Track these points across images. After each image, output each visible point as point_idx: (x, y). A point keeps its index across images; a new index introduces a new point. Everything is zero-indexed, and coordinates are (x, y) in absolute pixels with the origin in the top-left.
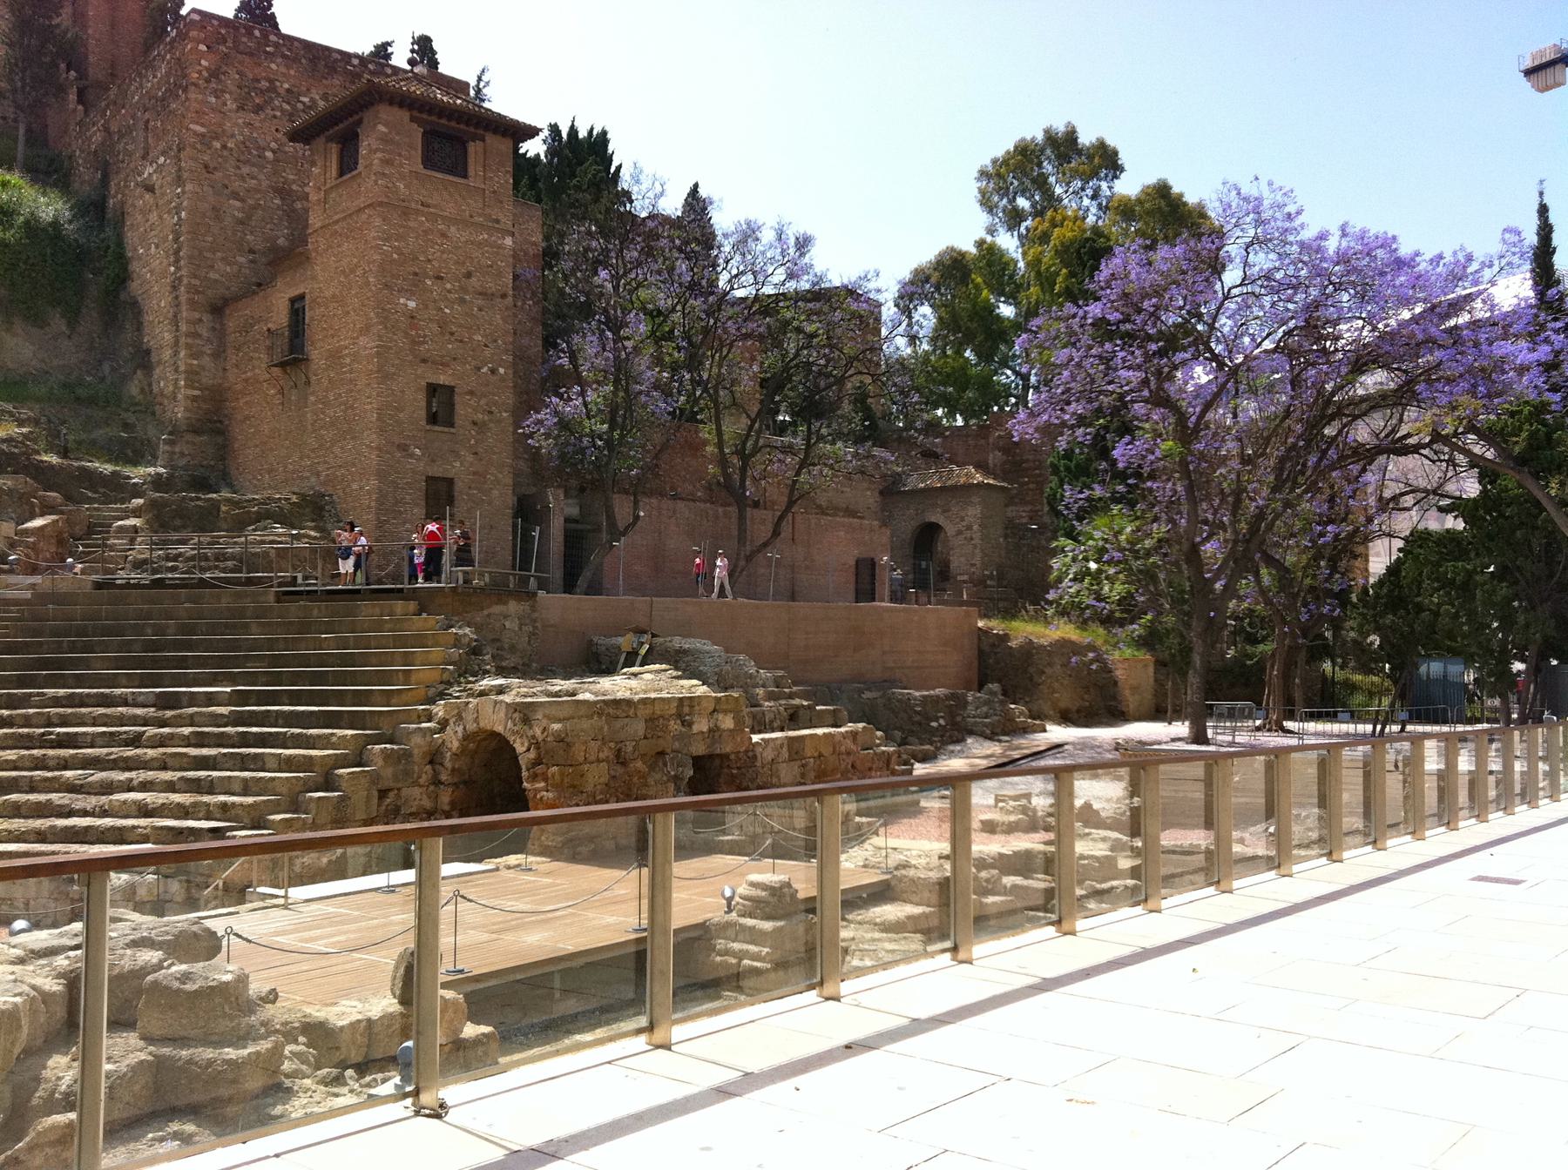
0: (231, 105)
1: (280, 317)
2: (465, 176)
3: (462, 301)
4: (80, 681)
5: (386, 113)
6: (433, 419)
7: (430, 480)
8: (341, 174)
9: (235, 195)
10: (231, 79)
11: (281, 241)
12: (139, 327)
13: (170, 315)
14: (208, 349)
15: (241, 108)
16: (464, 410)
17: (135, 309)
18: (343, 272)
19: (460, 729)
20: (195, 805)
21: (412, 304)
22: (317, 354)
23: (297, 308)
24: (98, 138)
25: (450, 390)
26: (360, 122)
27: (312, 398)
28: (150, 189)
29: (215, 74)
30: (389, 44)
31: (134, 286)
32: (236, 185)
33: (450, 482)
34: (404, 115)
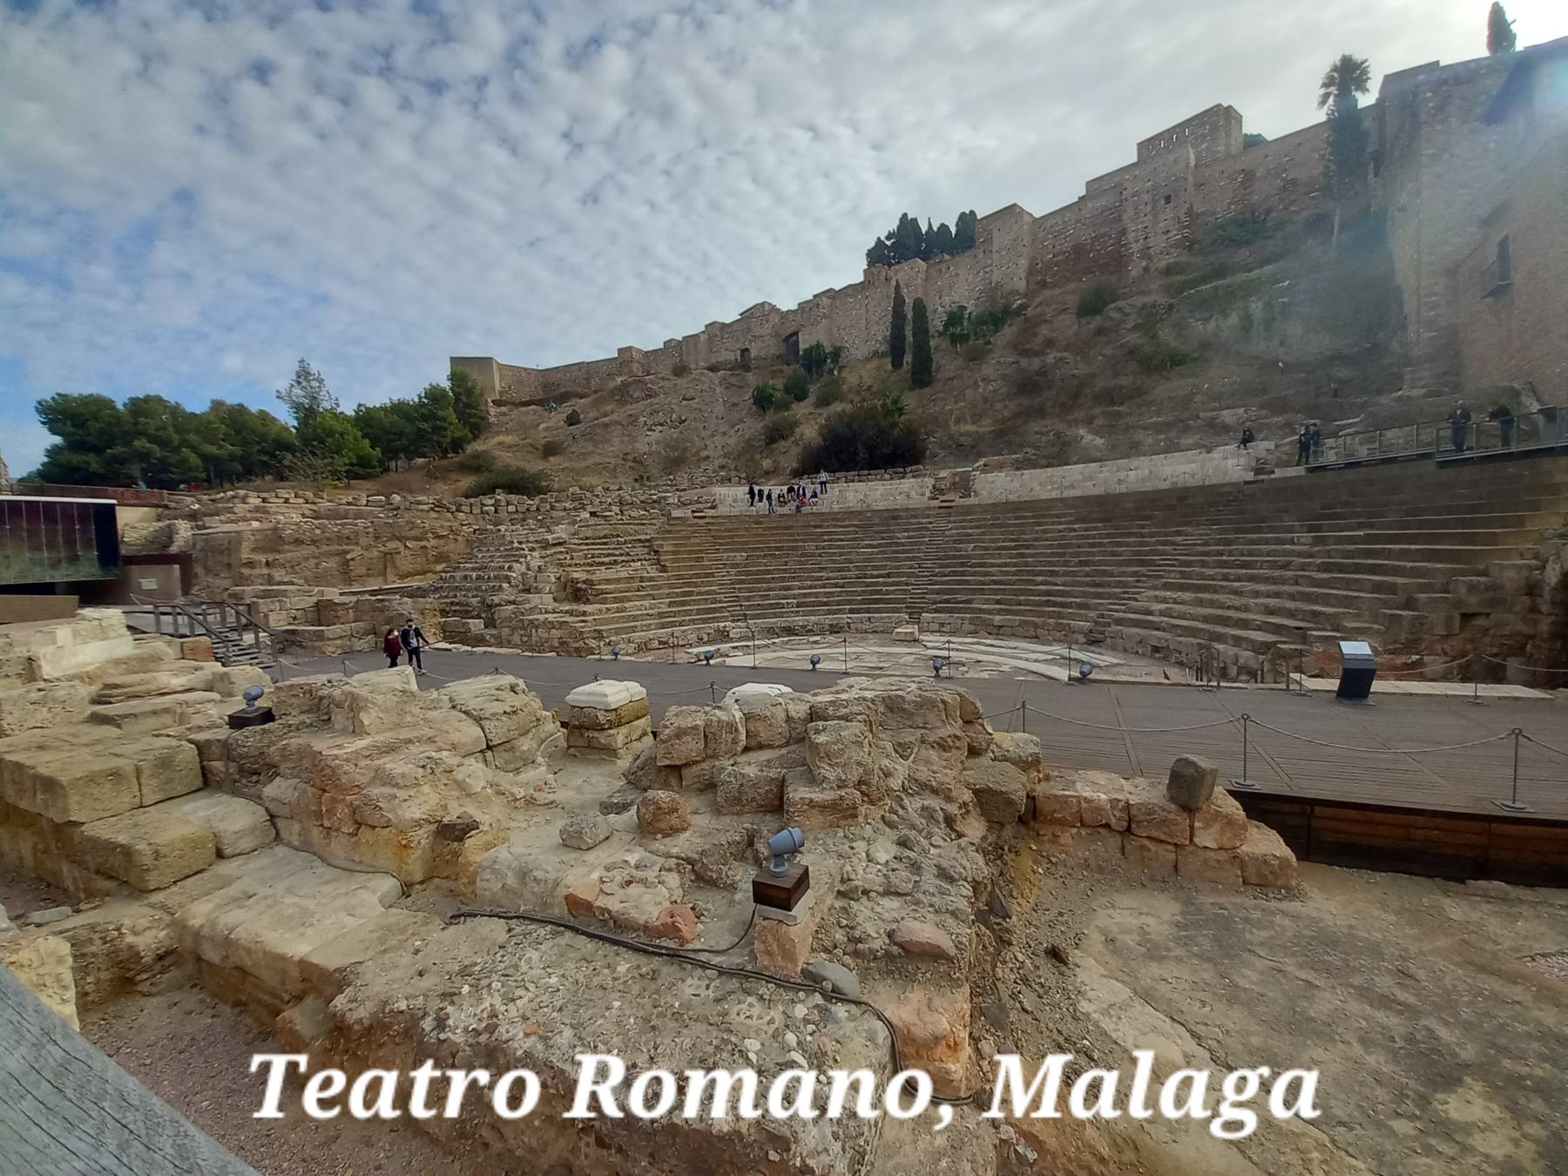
4: (1271, 530)
20: (1297, 610)
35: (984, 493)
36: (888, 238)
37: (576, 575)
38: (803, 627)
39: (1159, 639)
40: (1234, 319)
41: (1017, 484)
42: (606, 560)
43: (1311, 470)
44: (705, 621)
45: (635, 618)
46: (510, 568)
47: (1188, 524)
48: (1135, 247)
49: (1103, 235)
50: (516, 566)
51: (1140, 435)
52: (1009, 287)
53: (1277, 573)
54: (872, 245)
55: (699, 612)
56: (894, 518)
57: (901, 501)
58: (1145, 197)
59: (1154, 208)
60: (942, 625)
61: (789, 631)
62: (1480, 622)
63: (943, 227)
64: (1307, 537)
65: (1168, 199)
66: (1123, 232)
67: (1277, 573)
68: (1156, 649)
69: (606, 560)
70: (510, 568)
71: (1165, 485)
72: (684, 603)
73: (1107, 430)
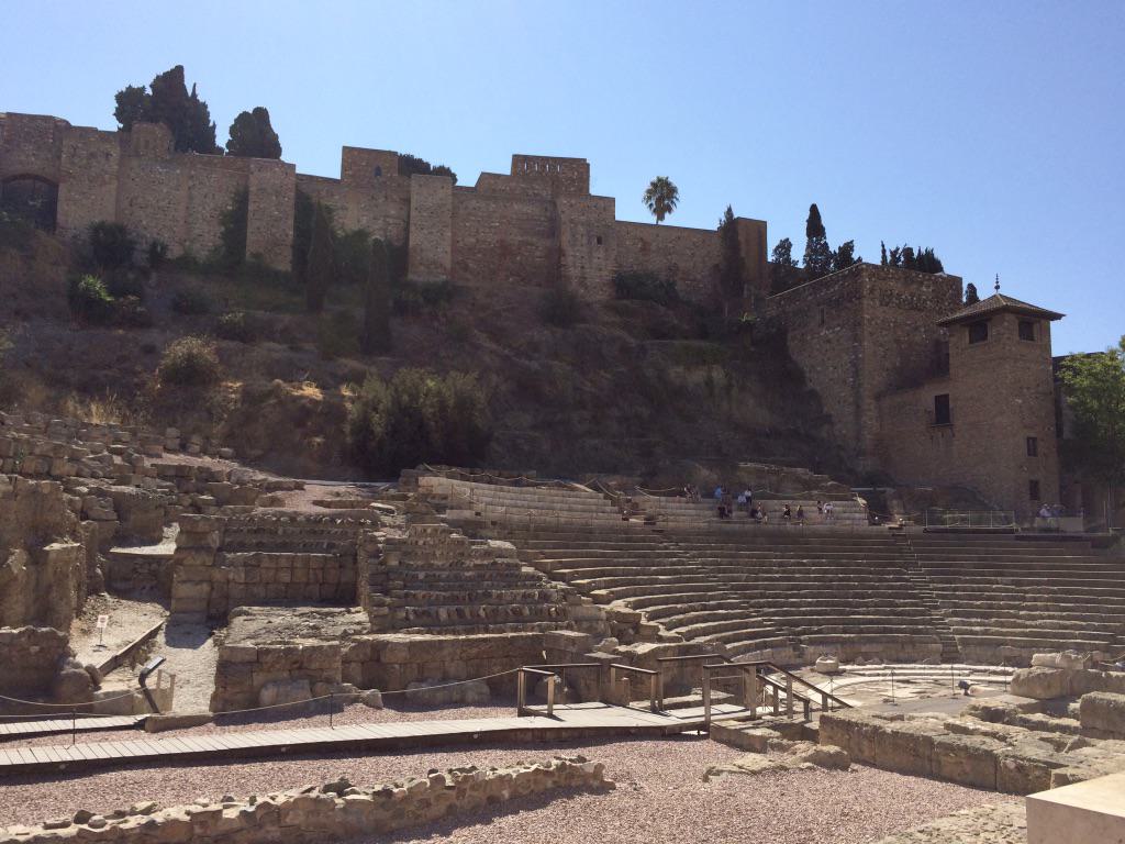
0: (878, 303)
1: (932, 407)
2: (1032, 340)
5: (1009, 317)
7: (1031, 482)
8: (971, 342)
9: (881, 345)
10: (877, 293)
13: (851, 400)
15: (881, 305)
18: (980, 387)
21: (1020, 401)
23: (942, 403)
24: (774, 313)
25: (1034, 439)
26: (989, 320)
27: (957, 443)
28: (829, 341)
29: (872, 291)
30: (852, 242)
31: (810, 385)
48: (574, 272)
49: (532, 245)
58: (581, 229)
59: (589, 242)
65: (599, 241)
66: (561, 252)
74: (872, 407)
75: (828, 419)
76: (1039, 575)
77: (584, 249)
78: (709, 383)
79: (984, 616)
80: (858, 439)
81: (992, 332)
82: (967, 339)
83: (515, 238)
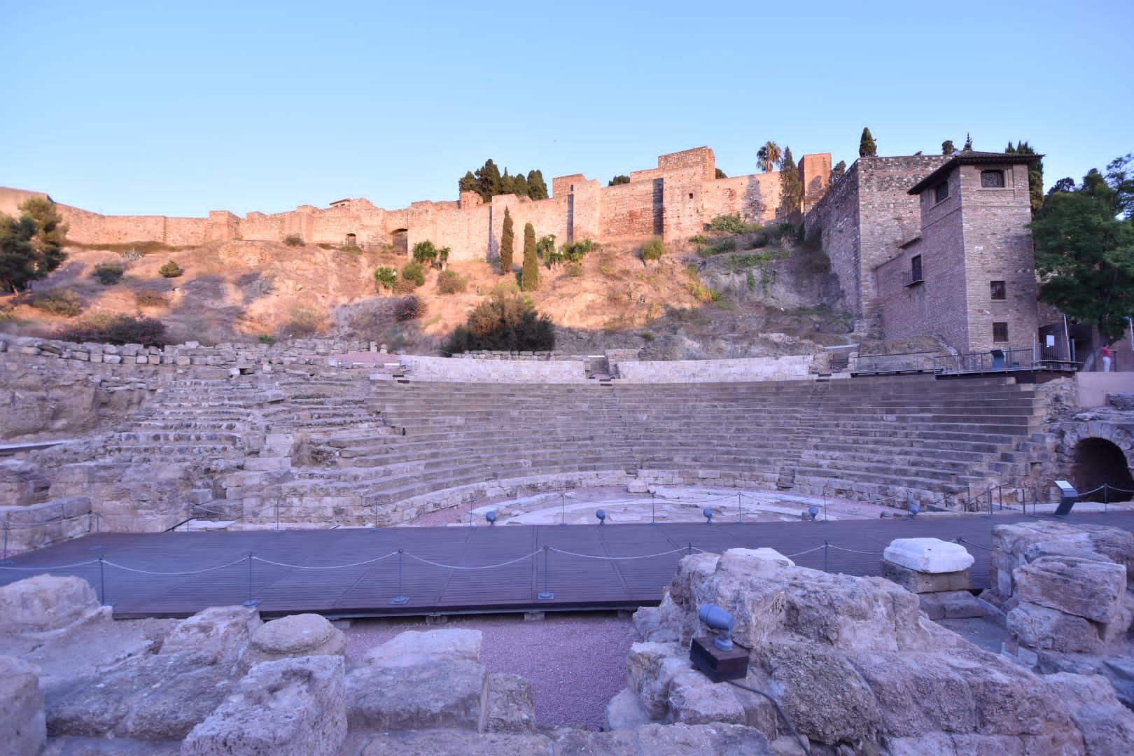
1: (907, 265)
3: (1006, 242)
5: (962, 169)
6: (995, 296)
10: (874, 181)
11: (899, 238)
12: (838, 283)
14: (871, 286)
16: (1009, 291)
17: (835, 277)
19: (1075, 437)
22: (928, 278)
25: (1002, 283)
28: (841, 231)
29: (867, 180)
31: (834, 269)
32: (879, 220)
33: (1005, 325)
34: (971, 169)
35: (630, 376)
36: (477, 173)
37: (314, 436)
38: (545, 484)
39: (843, 485)
40: (744, 277)
41: (653, 371)
42: (338, 420)
43: (853, 376)
44: (466, 481)
45: (404, 481)
46: (231, 427)
47: (797, 405)
50: (238, 425)
51: (723, 344)
52: (585, 230)
53: (888, 439)
54: (464, 175)
55: (456, 473)
56: (570, 391)
57: (566, 379)
58: (678, 192)
60: (656, 478)
61: (533, 489)
62: (1037, 467)
63: (520, 176)
64: (891, 417)
65: (691, 195)
67: (888, 439)
68: (839, 492)
69: (338, 420)
70: (231, 427)
71: (760, 379)
72: (437, 464)
73: (701, 337)
74: (869, 278)
75: (842, 294)
76: (930, 411)
77: (680, 205)
78: (750, 277)
79: (842, 449)
80: (858, 305)
81: (951, 187)
82: (934, 200)
83: (638, 207)
